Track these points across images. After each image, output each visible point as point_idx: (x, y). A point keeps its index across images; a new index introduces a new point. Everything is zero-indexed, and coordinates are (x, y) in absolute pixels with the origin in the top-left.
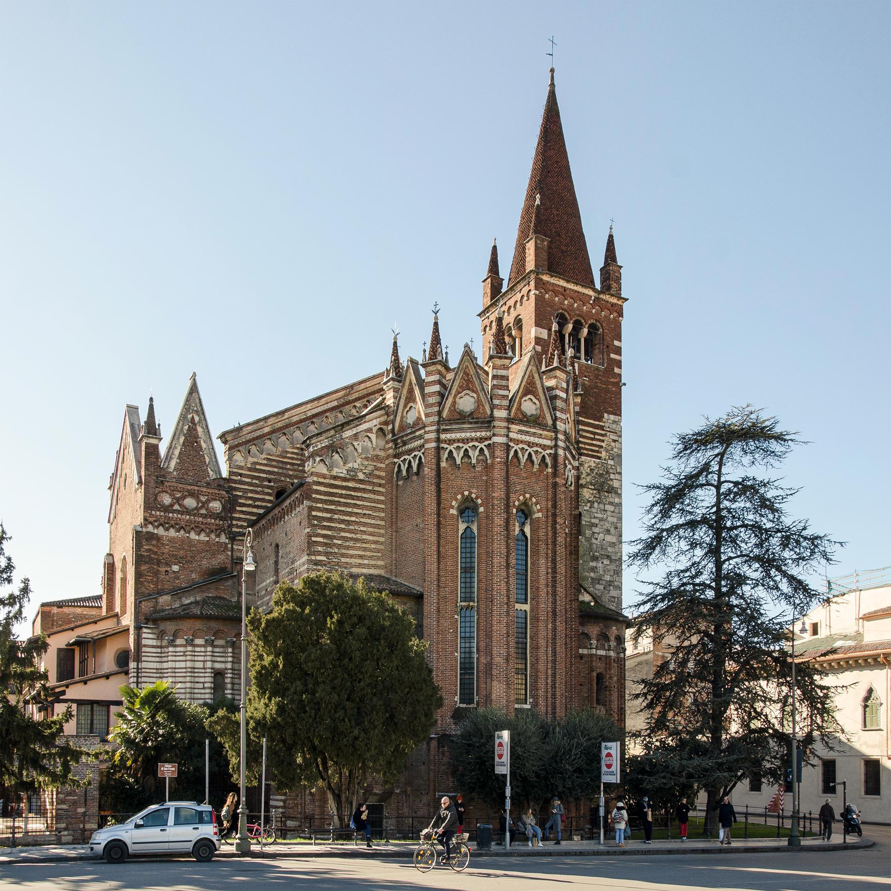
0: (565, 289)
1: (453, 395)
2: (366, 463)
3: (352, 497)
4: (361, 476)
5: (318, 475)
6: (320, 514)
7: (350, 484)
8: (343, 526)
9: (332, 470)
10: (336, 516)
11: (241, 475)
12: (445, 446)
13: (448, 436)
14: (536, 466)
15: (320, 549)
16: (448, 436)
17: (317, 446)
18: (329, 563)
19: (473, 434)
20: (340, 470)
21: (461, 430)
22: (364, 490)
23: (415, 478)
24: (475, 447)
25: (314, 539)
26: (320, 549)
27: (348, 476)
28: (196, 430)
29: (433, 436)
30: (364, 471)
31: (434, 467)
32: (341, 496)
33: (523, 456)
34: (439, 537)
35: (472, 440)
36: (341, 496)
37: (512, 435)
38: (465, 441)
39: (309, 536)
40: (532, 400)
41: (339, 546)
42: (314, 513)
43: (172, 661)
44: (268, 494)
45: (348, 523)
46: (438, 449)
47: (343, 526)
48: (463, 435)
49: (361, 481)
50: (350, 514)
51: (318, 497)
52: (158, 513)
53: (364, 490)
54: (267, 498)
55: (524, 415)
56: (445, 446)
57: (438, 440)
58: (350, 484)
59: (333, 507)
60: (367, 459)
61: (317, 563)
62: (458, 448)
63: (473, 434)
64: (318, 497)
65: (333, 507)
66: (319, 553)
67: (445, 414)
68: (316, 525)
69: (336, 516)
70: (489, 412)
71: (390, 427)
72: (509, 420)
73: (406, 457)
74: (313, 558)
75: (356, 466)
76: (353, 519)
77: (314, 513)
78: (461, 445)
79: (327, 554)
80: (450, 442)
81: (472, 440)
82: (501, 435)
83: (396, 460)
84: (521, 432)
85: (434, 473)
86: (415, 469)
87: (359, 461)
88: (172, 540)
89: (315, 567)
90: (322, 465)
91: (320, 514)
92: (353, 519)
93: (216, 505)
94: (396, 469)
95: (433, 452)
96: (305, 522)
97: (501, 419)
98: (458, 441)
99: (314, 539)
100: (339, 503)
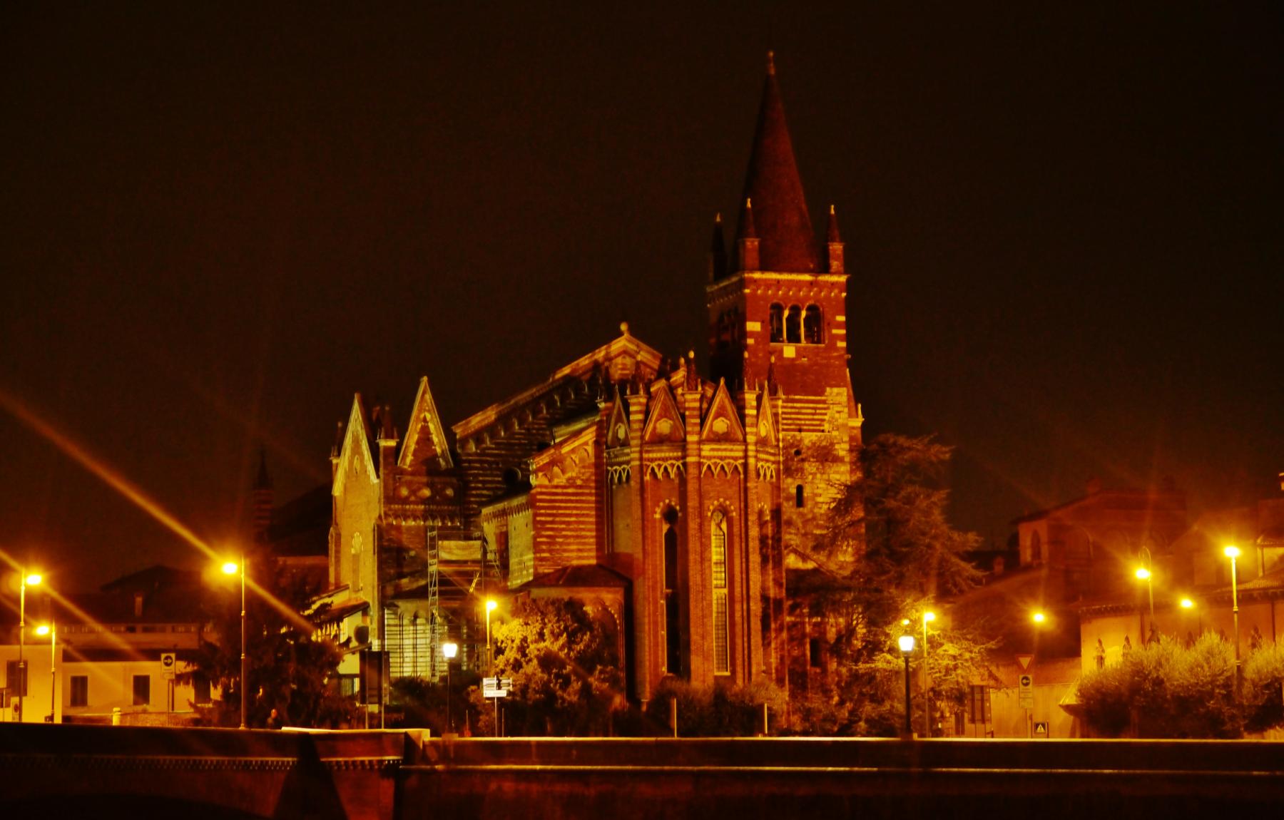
0: (778, 281)
1: (653, 422)
2: (583, 470)
3: (571, 501)
4: (579, 482)
5: (540, 486)
6: (543, 519)
7: (570, 491)
8: (563, 526)
9: (553, 480)
10: (557, 519)
11: (470, 462)
12: (648, 463)
13: (651, 455)
14: (729, 476)
15: (544, 547)
16: (651, 455)
17: (539, 464)
18: (553, 558)
19: (671, 454)
20: (561, 480)
21: (661, 451)
22: (582, 494)
23: (625, 486)
24: (673, 465)
25: (538, 540)
26: (544, 547)
27: (567, 484)
28: (428, 427)
29: (636, 455)
30: (582, 478)
31: (639, 481)
32: (561, 501)
33: (716, 469)
34: (644, 538)
35: (671, 459)
36: (561, 501)
37: (703, 453)
38: (665, 459)
39: (535, 538)
40: (723, 421)
41: (561, 544)
42: (538, 519)
43: (422, 638)
44: (497, 476)
45: (568, 523)
46: (641, 466)
47: (563, 526)
48: (663, 455)
49: (580, 487)
50: (570, 515)
51: (541, 504)
52: (396, 506)
53: (582, 494)
54: (496, 479)
55: (716, 434)
56: (648, 463)
57: (641, 459)
58: (570, 491)
59: (554, 512)
60: (584, 467)
61: (542, 559)
62: (659, 466)
63: (671, 454)
64: (541, 504)
65: (554, 512)
66: (544, 551)
67: (647, 437)
68: (540, 528)
69: (557, 519)
70: (683, 436)
71: (604, 440)
72: (700, 442)
73: (618, 467)
74: (538, 555)
75: (574, 475)
76: (573, 519)
77: (538, 519)
78: (661, 462)
79: (550, 551)
80: (652, 460)
81: (671, 459)
82: (693, 456)
83: (609, 468)
84: (713, 450)
85: (638, 486)
86: (624, 479)
87: (577, 470)
88: (409, 529)
89: (540, 563)
90: (544, 478)
91: (543, 519)
92: (573, 519)
93: (449, 492)
94: (610, 476)
95: (638, 469)
96: (530, 526)
97: (693, 443)
98: (659, 459)
99: (538, 540)
100: (560, 508)
